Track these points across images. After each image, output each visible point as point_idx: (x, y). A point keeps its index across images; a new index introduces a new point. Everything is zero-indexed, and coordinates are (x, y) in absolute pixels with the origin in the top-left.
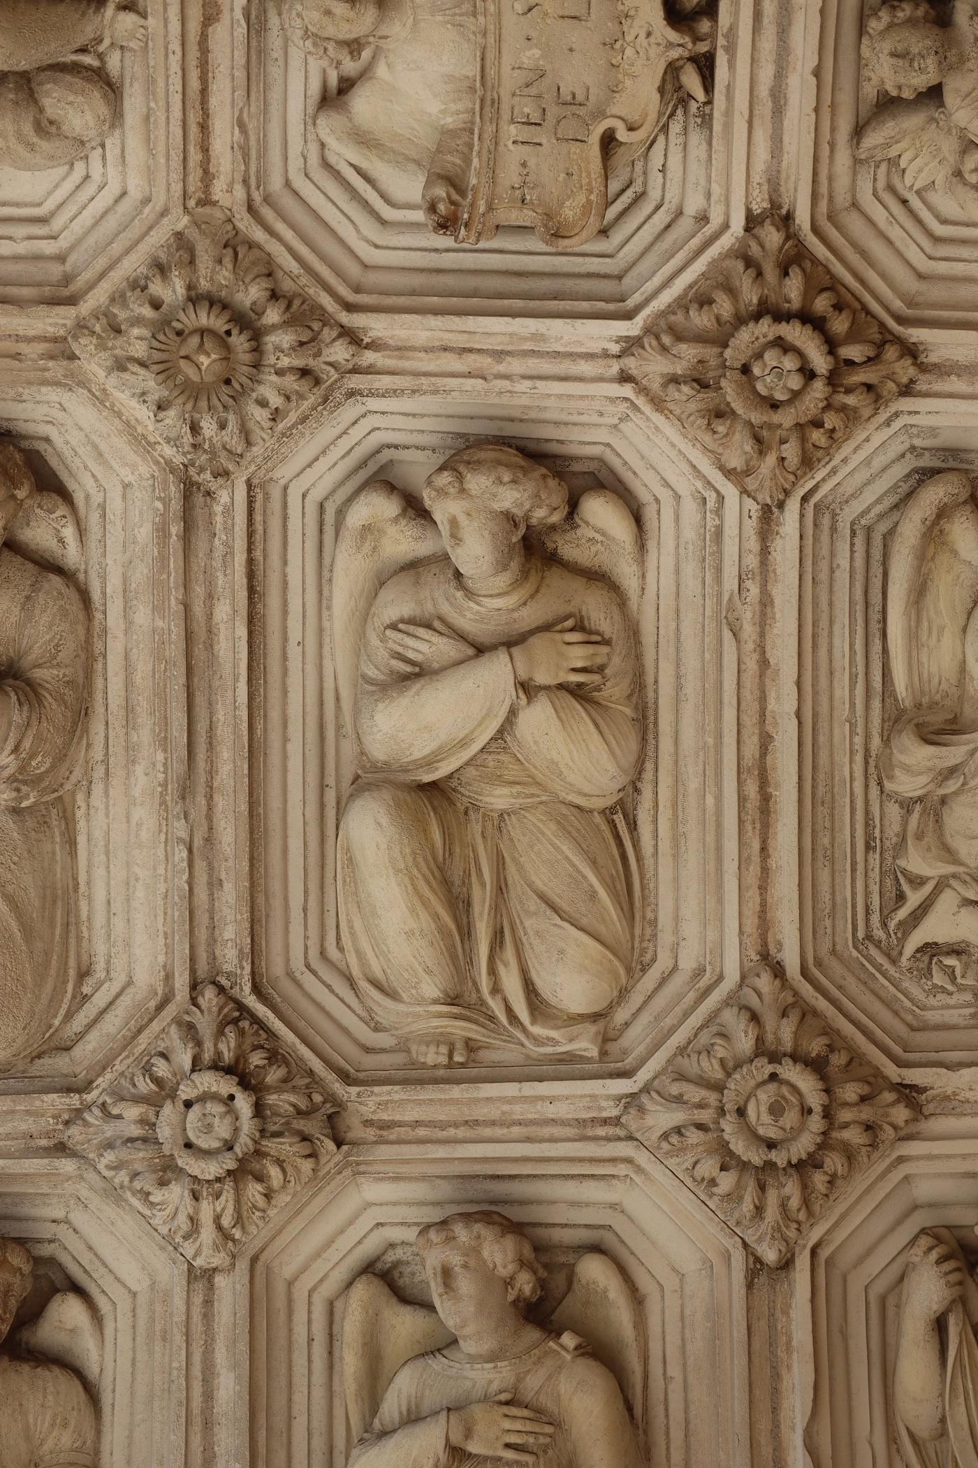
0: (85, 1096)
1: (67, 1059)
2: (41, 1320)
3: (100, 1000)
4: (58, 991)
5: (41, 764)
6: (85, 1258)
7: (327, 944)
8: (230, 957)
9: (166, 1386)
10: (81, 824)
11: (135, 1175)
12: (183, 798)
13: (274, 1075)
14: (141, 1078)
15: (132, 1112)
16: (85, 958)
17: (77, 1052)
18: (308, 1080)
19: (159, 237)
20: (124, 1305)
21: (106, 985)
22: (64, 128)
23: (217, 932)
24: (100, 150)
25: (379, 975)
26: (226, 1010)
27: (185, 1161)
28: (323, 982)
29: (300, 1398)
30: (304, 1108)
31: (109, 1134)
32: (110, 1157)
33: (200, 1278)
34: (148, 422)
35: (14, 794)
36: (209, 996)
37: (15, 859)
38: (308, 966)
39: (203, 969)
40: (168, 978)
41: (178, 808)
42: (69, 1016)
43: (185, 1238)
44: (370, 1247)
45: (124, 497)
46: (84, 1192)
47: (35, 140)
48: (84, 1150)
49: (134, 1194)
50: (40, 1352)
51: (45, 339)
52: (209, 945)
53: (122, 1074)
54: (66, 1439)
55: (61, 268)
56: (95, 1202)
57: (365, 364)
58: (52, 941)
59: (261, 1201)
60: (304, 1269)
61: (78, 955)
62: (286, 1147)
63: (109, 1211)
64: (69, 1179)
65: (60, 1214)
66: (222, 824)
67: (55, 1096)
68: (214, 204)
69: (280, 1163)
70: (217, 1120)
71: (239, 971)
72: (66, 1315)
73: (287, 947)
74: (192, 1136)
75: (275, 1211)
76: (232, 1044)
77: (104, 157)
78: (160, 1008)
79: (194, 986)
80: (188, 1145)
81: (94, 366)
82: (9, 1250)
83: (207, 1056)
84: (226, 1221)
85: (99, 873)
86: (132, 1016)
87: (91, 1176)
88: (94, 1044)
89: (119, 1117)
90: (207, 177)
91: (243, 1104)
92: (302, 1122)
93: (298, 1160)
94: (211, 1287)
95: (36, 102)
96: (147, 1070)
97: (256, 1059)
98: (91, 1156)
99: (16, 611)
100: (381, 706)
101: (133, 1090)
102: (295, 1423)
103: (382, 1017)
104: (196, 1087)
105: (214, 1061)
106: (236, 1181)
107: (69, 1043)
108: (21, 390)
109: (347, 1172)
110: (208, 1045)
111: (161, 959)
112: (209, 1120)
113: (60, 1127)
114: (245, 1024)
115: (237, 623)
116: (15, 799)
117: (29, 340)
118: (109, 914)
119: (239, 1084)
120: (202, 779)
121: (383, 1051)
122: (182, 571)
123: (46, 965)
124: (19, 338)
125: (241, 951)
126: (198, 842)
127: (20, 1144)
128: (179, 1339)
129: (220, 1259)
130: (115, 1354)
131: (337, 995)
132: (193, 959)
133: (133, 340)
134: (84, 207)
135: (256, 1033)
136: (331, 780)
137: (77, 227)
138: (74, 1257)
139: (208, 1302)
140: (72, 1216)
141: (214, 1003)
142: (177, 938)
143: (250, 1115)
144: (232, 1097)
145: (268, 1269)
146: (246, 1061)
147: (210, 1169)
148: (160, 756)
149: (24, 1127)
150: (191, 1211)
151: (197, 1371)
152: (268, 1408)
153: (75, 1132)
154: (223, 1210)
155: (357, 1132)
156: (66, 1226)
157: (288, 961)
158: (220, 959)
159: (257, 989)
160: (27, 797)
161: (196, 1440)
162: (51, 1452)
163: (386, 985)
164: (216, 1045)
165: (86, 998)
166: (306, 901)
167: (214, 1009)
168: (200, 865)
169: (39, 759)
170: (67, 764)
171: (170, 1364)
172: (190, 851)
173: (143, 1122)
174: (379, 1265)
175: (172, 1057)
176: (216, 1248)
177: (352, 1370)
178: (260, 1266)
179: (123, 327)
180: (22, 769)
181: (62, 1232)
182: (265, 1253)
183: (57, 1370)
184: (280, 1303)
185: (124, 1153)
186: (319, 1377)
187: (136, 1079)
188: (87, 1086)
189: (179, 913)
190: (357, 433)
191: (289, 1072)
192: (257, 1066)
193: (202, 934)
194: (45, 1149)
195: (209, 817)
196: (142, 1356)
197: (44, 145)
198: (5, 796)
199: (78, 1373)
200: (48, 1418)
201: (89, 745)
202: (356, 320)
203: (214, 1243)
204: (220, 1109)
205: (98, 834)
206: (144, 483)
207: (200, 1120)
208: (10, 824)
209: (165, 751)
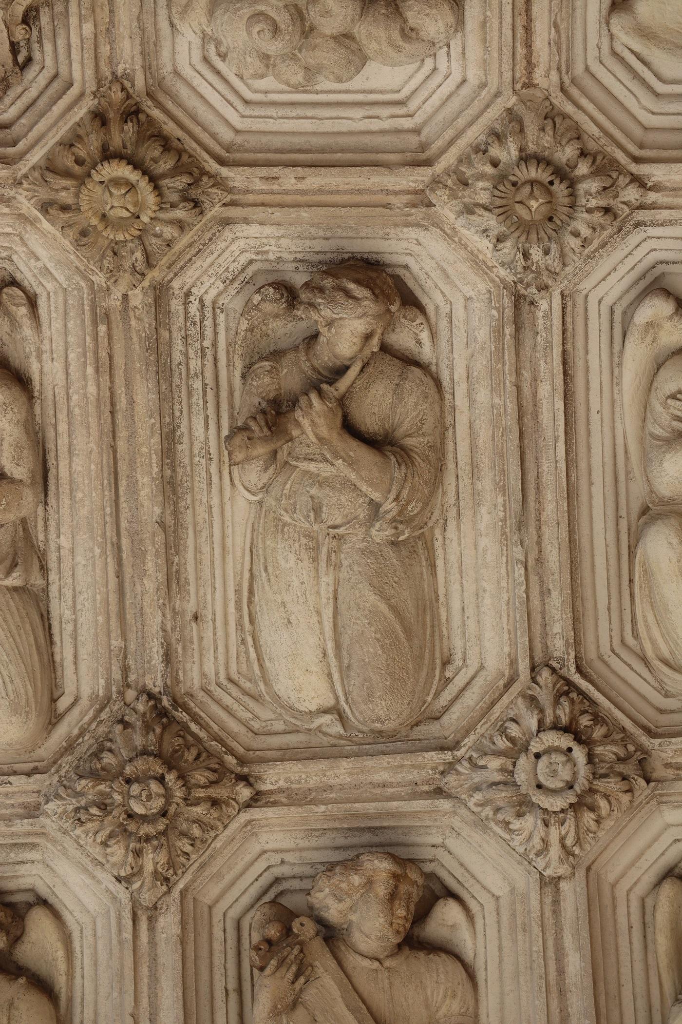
0: (456, 753)
1: (438, 726)
2: (429, 919)
3: (460, 681)
4: (431, 675)
5: (414, 508)
6: (459, 872)
7: (625, 634)
8: (558, 647)
9: (528, 965)
10: (439, 552)
11: (497, 810)
12: (519, 530)
13: (598, 732)
14: (499, 738)
15: (495, 763)
16: (446, 650)
17: (445, 720)
18: (622, 735)
19: (495, 112)
20: (490, 906)
21: (464, 670)
22: (422, 33)
23: (548, 628)
24: (445, 49)
25: (666, 654)
26: (558, 686)
27: (538, 798)
28: (625, 662)
29: (625, 970)
30: (623, 756)
31: (476, 780)
32: (478, 797)
33: (550, 884)
34: (487, 251)
35: (393, 531)
36: (545, 675)
37: (396, 579)
38: (613, 651)
39: (539, 656)
40: (513, 663)
41: (516, 538)
42: (437, 695)
43: (538, 854)
44: (670, 857)
45: (466, 307)
46: (457, 823)
47: (401, 43)
48: (458, 792)
49: (496, 824)
50: (428, 943)
51: (408, 192)
52: (542, 638)
53: (482, 735)
54: (455, 1006)
55: (418, 138)
56: (466, 831)
57: (649, 202)
58: (425, 639)
59: (593, 826)
60: (623, 875)
61: (441, 649)
62: (612, 785)
63: (477, 837)
64: (446, 814)
65: (438, 840)
66: (549, 548)
67: (433, 753)
68: (535, 86)
69: (606, 797)
70: (560, 767)
71: (566, 657)
72: (448, 914)
73: (597, 637)
74: (542, 779)
75: (603, 833)
76: (567, 711)
77: (449, 54)
78: (508, 686)
79: (533, 668)
80: (539, 786)
81: (447, 210)
82: (408, 869)
83: (549, 720)
84: (569, 842)
85: (455, 587)
86: (486, 693)
87: (463, 811)
88: (458, 714)
89: (484, 767)
90: (530, 66)
91: (579, 754)
92: (622, 766)
93: (620, 794)
94: (557, 891)
95: (401, 15)
96: (503, 731)
97: (585, 721)
98: (463, 797)
99: (389, 395)
100: (668, 456)
101: (493, 747)
102: (623, 989)
103: (671, 687)
104: (543, 743)
105: (554, 723)
106: (575, 812)
107: (438, 714)
108: (388, 230)
109: (654, 802)
110: (549, 712)
111: (507, 649)
112: (554, 767)
113: (438, 776)
114: (574, 695)
115: (556, 399)
116: (394, 535)
117: (396, 193)
118: (464, 618)
119: (575, 739)
120: (533, 515)
121: (673, 711)
122: (514, 361)
123: (422, 657)
124: (388, 192)
125: (567, 641)
126: (531, 562)
127: (408, 790)
128: (536, 930)
129: (563, 870)
130: (485, 943)
131: (636, 672)
132: (531, 649)
133: (478, 191)
134: (434, 92)
135: (582, 702)
136: (623, 512)
137: (428, 107)
138: (449, 872)
139: (556, 902)
140: (447, 842)
141: (550, 680)
142: (519, 633)
143: (585, 762)
144: (570, 750)
145: (598, 876)
146: (577, 722)
147: (557, 803)
148: (500, 499)
149: (410, 777)
150: (543, 834)
151: (551, 953)
152: (605, 979)
153: (451, 779)
154: (567, 833)
155: (660, 772)
156: (443, 849)
157: (598, 647)
158: (551, 648)
159: (579, 669)
160: (403, 533)
161: (554, 1004)
162: (445, 1016)
163: (673, 663)
164: (554, 711)
165: (449, 680)
166: (609, 602)
167: (550, 685)
168: (534, 579)
169: (414, 504)
170: (429, 507)
171: (531, 950)
172: (526, 569)
173: (502, 770)
174: (677, 871)
175: (521, 721)
176: (561, 861)
177: (664, 948)
178: (592, 872)
179: (470, 181)
180: (400, 513)
181: (440, 853)
182: (596, 864)
183: (444, 956)
184: (607, 901)
185: (491, 794)
186: (638, 955)
187: (495, 739)
188: (456, 746)
189: (520, 616)
190: (639, 254)
191: (609, 730)
192: (586, 726)
193: (537, 630)
194: (427, 793)
195: (539, 543)
196: (507, 943)
197: (407, 46)
198: (387, 533)
199: (458, 957)
200: (441, 991)
201: (444, 493)
202: (642, 170)
203: (560, 858)
204: (563, 758)
205: (453, 558)
206: (482, 297)
207: (547, 767)
208: (390, 553)
209: (504, 495)
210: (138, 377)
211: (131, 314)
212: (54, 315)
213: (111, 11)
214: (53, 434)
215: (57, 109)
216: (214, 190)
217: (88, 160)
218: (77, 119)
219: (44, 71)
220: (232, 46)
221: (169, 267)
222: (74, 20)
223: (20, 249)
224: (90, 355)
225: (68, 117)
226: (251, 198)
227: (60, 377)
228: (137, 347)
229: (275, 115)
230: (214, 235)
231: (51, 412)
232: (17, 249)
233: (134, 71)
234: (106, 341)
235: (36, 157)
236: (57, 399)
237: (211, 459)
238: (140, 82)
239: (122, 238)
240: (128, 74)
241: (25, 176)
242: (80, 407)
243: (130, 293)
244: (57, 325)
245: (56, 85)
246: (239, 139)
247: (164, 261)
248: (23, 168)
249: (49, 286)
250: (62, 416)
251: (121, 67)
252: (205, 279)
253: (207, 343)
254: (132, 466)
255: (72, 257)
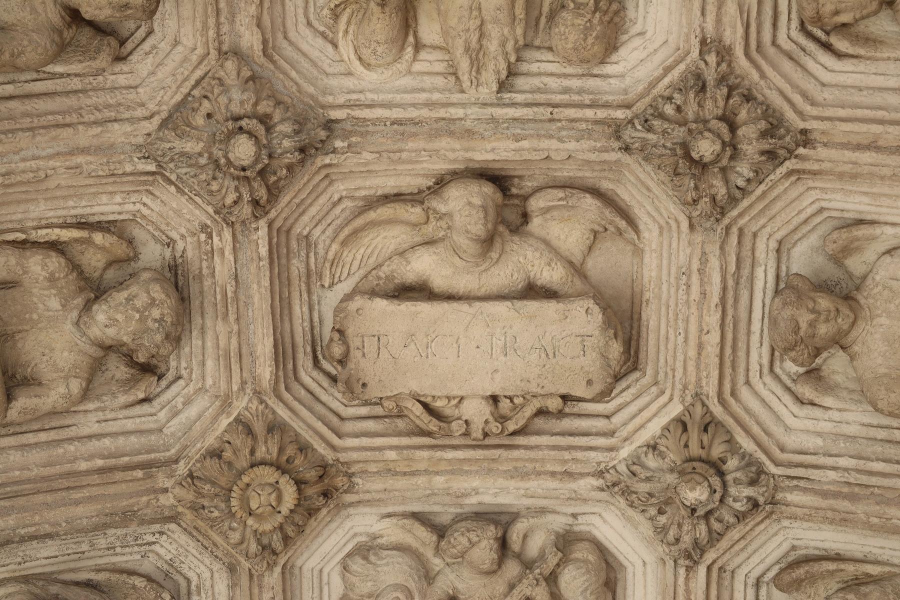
210: (99, 507)
211: (152, 497)
212: (138, 420)
213: (405, 474)
214: (35, 428)
215: (319, 426)
216: (265, 565)
217: (291, 466)
218: (316, 446)
219: (343, 407)
220: (379, 569)
221: (195, 528)
222: (395, 441)
223: (191, 389)
224: (112, 462)
225: (317, 438)
226: (256, 591)
227: (86, 431)
228: (125, 503)
229: (315, 595)
230: (221, 559)
231: (53, 424)
232: (191, 385)
233: (357, 493)
234: (130, 478)
235: (283, 413)
236: (66, 429)
237: (20, 564)
238: (349, 498)
239: (233, 504)
240: (354, 487)
241: (267, 406)
242: (65, 453)
243: (170, 494)
244: (130, 425)
245: (335, 420)
246: (297, 571)
247: (200, 523)
248: (272, 402)
249: (162, 415)
250: (53, 435)
251: (359, 481)
252: (175, 546)
253: (118, 550)
254: (23, 509)
255: (199, 445)
